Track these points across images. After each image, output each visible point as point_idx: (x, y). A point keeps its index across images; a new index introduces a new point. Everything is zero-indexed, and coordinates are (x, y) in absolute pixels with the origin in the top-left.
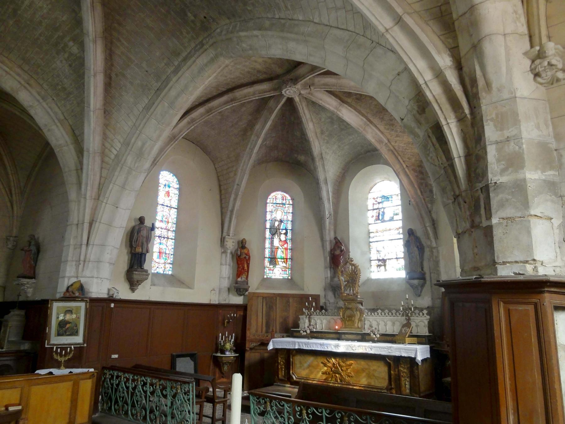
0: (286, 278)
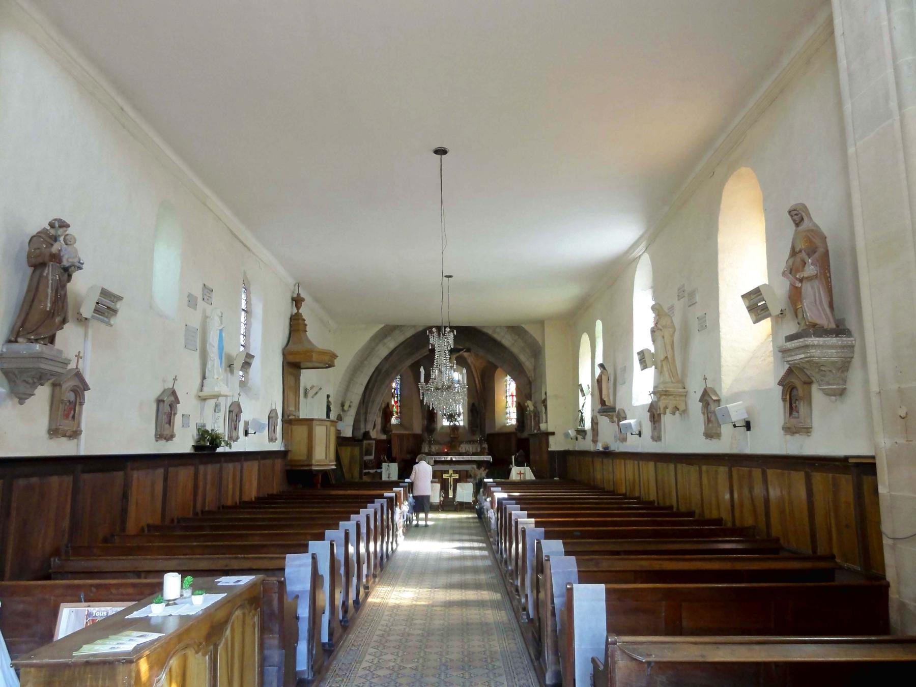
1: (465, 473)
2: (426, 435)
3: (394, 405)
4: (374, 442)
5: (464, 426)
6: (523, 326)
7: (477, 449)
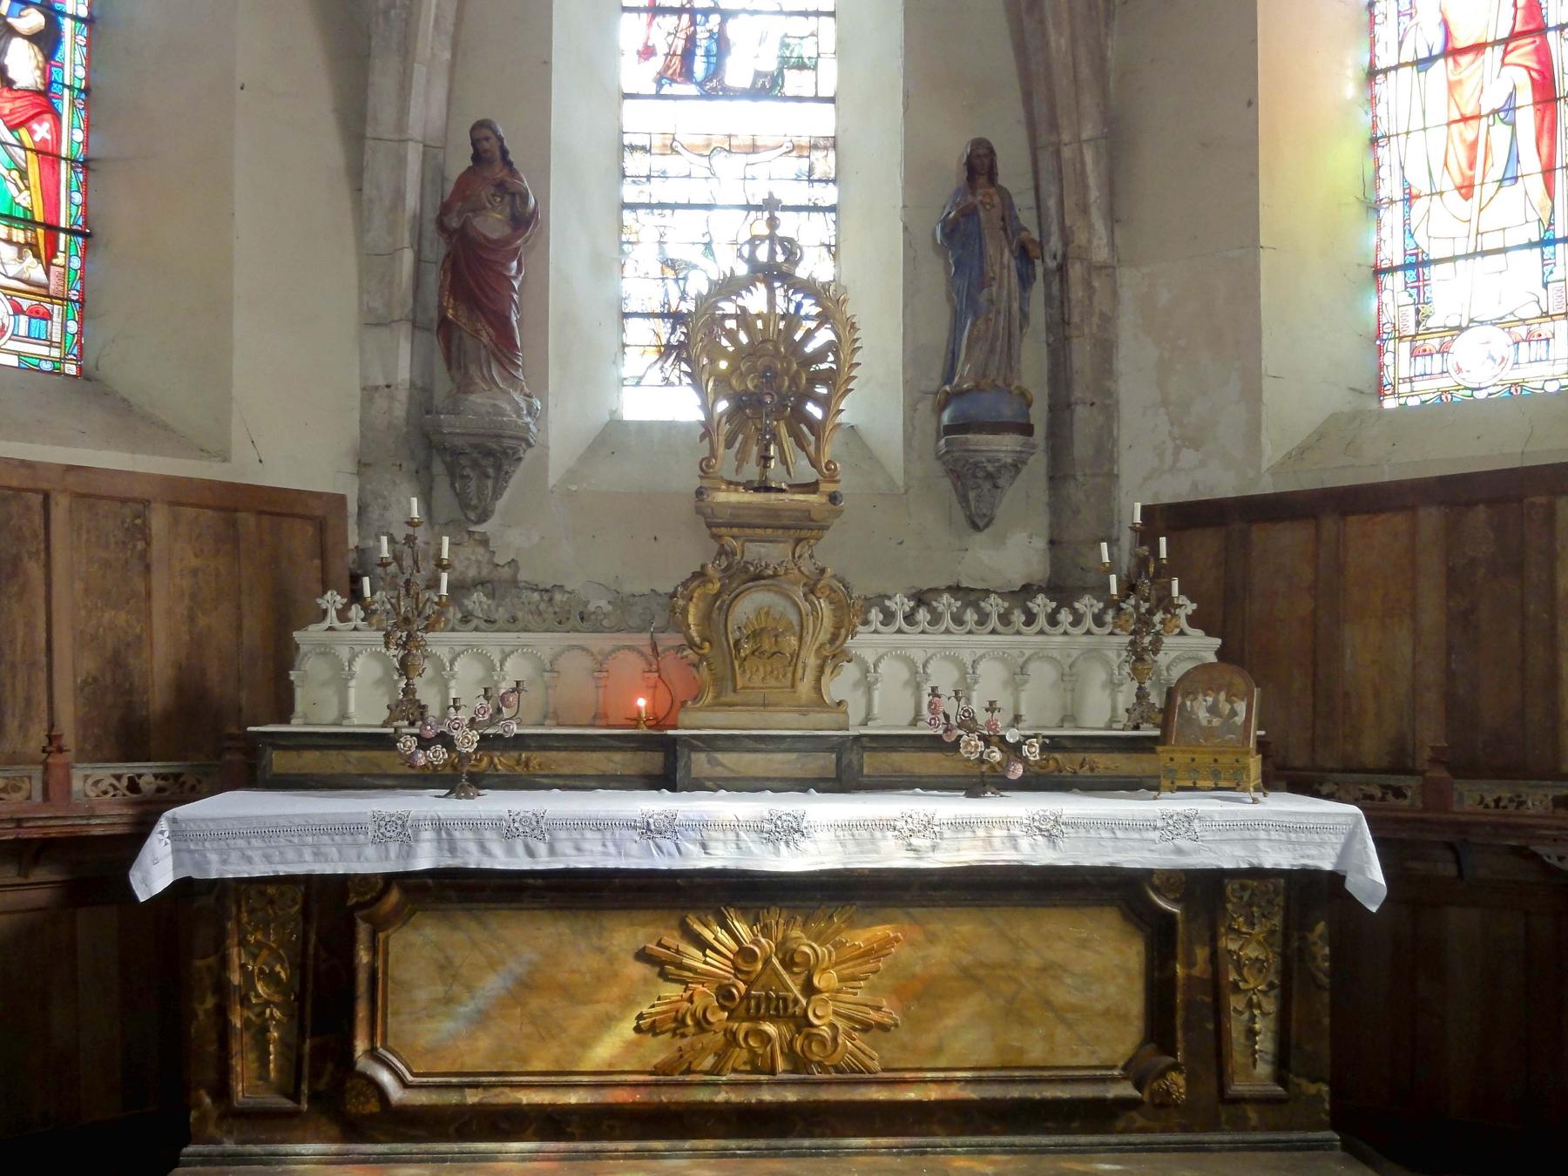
0: (46, 366)
7: (1069, 678)
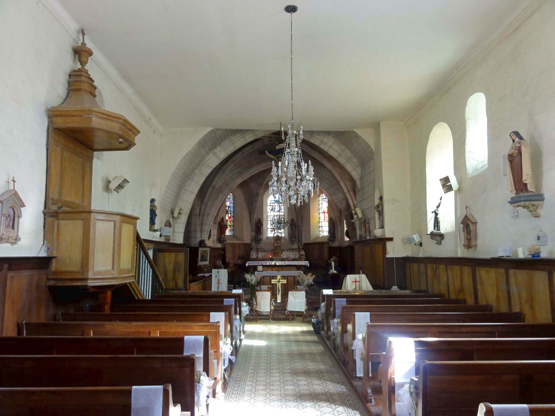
1: (293, 277)
2: (254, 244)
3: (228, 220)
4: (209, 249)
5: (284, 237)
6: (355, 130)
7: (296, 255)
